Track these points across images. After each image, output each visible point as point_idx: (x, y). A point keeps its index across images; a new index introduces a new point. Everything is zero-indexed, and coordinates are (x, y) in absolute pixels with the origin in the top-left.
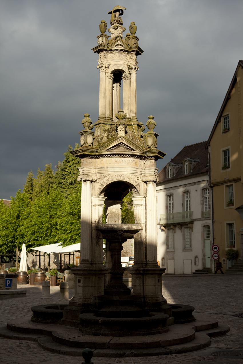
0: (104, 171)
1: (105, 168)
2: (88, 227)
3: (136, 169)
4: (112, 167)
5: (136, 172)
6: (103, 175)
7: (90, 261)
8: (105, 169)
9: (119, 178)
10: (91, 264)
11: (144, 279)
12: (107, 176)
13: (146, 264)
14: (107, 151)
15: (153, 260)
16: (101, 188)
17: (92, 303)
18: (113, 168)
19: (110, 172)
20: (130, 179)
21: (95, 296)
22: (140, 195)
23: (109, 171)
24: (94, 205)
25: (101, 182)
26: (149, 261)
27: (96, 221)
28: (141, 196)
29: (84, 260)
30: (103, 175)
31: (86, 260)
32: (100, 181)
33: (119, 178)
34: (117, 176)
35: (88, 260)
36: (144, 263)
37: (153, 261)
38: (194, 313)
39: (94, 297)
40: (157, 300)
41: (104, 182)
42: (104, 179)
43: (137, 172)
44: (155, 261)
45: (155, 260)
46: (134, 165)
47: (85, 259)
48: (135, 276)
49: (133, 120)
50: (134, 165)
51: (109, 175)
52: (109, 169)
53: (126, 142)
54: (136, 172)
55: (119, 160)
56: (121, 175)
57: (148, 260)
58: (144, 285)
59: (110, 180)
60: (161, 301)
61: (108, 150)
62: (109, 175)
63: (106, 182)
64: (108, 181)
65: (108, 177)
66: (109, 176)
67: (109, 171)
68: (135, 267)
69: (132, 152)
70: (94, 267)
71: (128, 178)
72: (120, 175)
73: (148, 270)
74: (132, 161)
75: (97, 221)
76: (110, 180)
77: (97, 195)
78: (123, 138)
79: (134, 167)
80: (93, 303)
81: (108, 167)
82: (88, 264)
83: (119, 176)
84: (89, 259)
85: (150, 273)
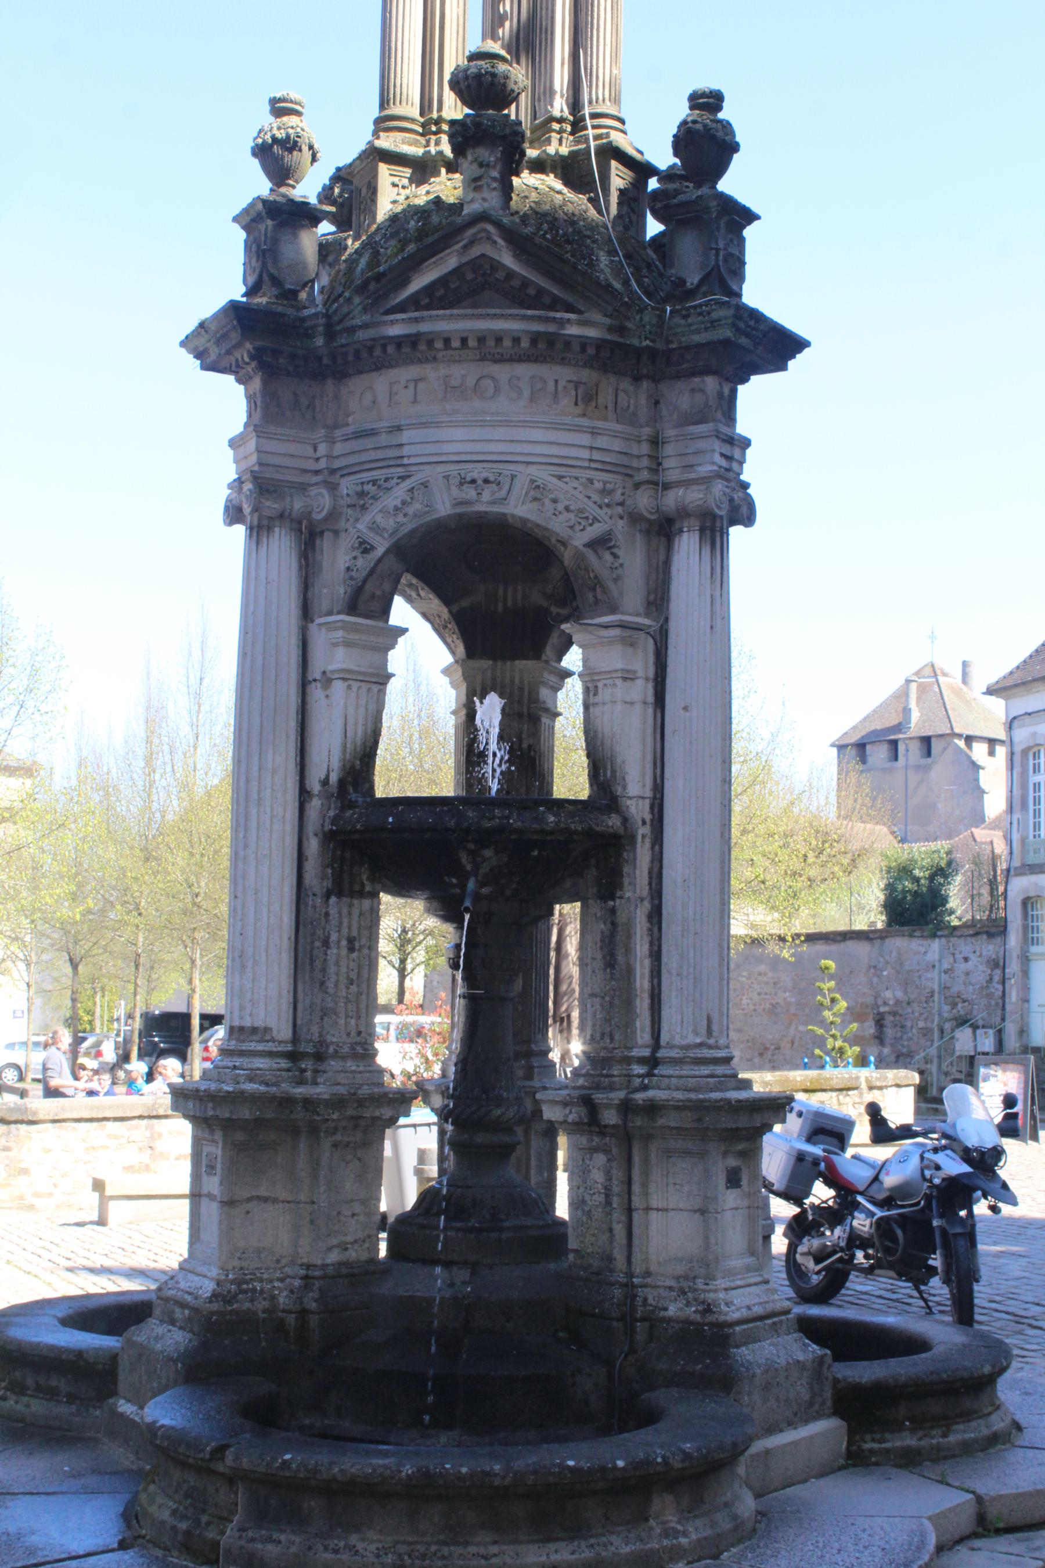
0: (380, 455)
1: (384, 436)
2: (272, 816)
3: (585, 439)
4: (425, 425)
5: (585, 454)
6: (374, 482)
7: (286, 1033)
8: (383, 439)
9: (470, 493)
10: (293, 1056)
11: (636, 1159)
12: (395, 481)
13: (653, 1062)
14: (391, 317)
15: (698, 1040)
16: (360, 562)
17: (284, 1311)
18: (434, 434)
19: (413, 460)
20: (547, 501)
21: (308, 1266)
22: (614, 610)
23: (406, 451)
24: (318, 677)
25: (361, 526)
26: (672, 1047)
27: (325, 783)
28: (623, 613)
29: (241, 1029)
30: (374, 482)
31: (254, 1030)
32: (357, 520)
33: (470, 493)
34: (457, 481)
35: (267, 1030)
36: (641, 1061)
37: (701, 1045)
38: (1006, 1390)
39: (302, 1272)
40: (708, 1309)
41: (375, 528)
42: (379, 505)
43: (596, 456)
44: (710, 1047)
45: (711, 1041)
46: (579, 410)
47: (247, 1023)
48: (584, 1140)
49: (594, 127)
50: (579, 410)
51: (409, 476)
52: (406, 436)
53: (516, 256)
54: (585, 454)
55: (471, 382)
56: (485, 475)
57: (664, 1038)
58: (637, 1201)
59: (416, 506)
60: (736, 1316)
61: (401, 308)
62: (403, 478)
63: (390, 523)
64: (400, 518)
65: (399, 493)
66: (407, 484)
67: (406, 451)
68: (581, 1081)
69: (554, 320)
70: (309, 1074)
71: (532, 493)
72: (478, 472)
73: (653, 1109)
74: (562, 383)
75: (334, 778)
76: (410, 510)
77: (339, 613)
78: (490, 228)
79: (568, 420)
80: (290, 1312)
81: (399, 428)
82: (271, 1054)
83: (473, 481)
84: (272, 1023)
85: (673, 1124)
